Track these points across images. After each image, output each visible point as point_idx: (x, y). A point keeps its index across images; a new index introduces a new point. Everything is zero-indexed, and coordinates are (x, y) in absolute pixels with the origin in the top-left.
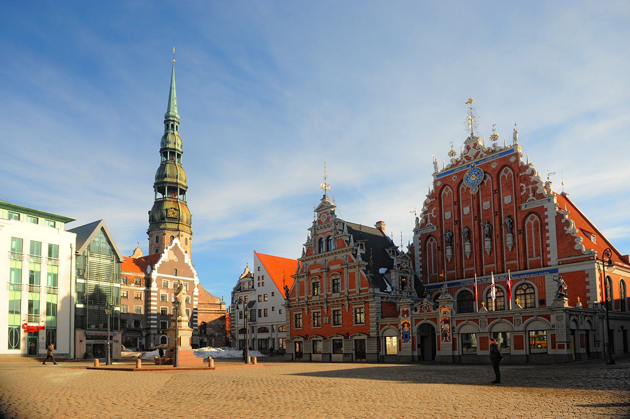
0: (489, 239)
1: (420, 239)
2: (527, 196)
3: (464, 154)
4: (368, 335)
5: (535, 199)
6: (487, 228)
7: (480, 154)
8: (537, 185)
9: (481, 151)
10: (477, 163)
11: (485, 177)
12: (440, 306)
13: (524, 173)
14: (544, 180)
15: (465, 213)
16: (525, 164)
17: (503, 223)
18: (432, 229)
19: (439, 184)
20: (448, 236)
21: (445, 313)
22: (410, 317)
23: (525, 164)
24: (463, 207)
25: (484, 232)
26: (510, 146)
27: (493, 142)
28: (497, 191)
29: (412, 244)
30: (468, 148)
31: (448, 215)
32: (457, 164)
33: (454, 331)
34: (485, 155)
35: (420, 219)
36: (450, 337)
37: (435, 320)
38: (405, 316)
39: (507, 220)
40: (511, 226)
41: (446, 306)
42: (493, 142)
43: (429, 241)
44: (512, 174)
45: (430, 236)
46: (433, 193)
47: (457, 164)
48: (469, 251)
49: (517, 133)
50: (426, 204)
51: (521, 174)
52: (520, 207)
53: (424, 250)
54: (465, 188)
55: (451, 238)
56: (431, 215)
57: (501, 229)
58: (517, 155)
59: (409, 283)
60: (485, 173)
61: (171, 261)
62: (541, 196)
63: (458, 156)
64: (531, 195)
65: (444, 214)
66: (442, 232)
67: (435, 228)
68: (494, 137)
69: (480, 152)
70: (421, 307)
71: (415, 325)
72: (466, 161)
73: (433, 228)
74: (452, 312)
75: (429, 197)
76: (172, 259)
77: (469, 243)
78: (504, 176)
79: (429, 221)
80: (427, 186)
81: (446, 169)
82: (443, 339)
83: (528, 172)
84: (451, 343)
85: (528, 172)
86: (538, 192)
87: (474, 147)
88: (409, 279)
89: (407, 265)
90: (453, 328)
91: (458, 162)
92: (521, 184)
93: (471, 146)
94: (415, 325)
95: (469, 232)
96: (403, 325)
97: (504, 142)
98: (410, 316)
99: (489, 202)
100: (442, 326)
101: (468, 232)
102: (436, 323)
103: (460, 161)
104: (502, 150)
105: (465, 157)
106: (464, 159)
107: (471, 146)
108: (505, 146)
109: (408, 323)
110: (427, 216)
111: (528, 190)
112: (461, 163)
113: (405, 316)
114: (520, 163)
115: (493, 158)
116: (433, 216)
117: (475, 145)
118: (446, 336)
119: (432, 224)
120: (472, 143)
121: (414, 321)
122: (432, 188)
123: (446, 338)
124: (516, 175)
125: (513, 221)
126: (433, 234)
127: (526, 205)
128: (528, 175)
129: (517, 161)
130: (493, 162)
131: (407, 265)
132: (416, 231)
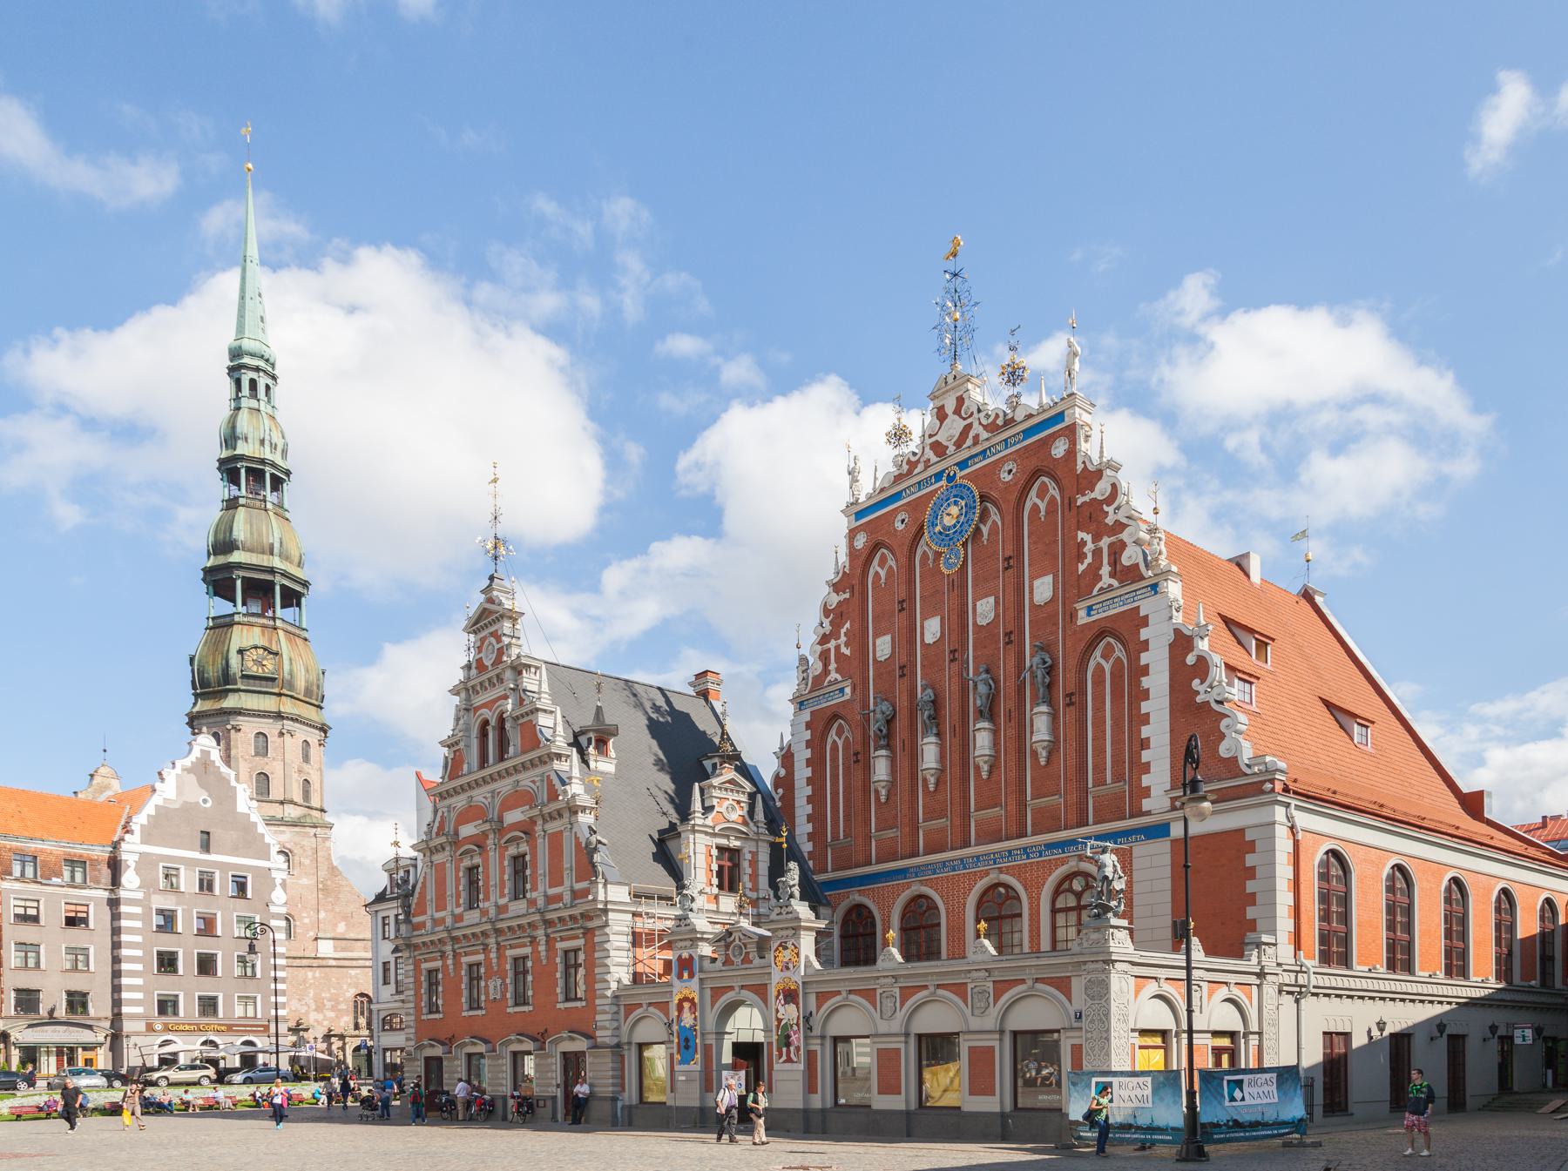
17: (1028, 664)
28: (1013, 562)
33: (811, 1029)
36: (798, 1049)
39: (1037, 660)
40: (1047, 680)
48: (934, 765)
60: (983, 498)
61: (188, 809)
82: (780, 1056)
84: (801, 1067)
90: (807, 1019)
99: (992, 600)
118: (788, 1045)
123: (788, 1052)
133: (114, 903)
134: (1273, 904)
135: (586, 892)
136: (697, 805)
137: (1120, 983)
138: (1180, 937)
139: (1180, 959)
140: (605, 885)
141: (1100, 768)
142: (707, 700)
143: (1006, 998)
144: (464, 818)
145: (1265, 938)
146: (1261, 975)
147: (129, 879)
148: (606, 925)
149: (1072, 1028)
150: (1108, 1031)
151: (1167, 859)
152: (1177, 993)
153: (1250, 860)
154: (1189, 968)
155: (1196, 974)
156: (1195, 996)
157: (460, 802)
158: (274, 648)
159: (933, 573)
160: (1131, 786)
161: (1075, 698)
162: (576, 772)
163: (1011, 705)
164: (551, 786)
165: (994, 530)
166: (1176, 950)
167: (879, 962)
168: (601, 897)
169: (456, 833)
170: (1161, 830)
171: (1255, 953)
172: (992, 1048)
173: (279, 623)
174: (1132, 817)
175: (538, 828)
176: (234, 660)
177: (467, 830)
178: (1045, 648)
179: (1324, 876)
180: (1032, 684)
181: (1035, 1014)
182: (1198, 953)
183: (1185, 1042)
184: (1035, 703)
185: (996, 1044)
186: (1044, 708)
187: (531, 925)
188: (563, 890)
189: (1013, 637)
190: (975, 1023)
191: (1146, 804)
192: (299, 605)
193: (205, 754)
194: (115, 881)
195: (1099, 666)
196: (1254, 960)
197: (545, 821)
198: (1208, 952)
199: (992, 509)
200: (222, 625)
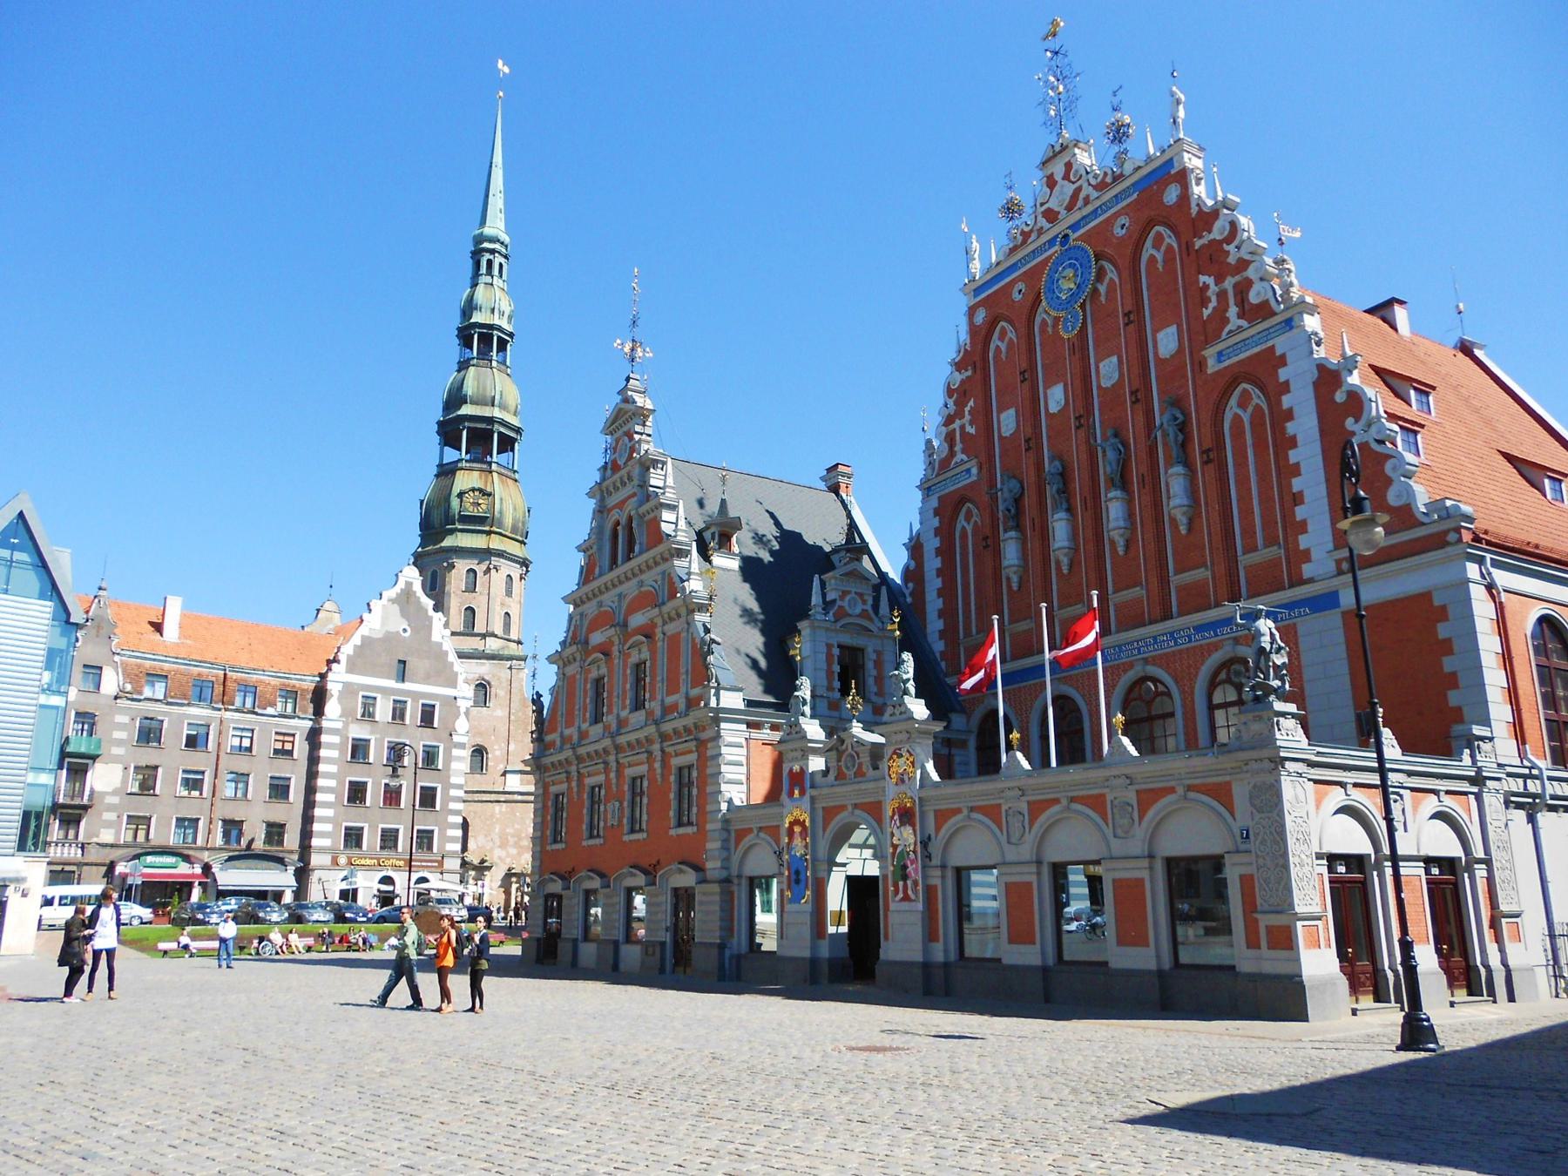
0: (1118, 493)
2: (1220, 317)
4: (699, 868)
5: (1244, 323)
6: (1111, 455)
7: (1082, 195)
8: (1251, 273)
12: (888, 751)
13: (1204, 241)
15: (1054, 408)
16: (1210, 203)
18: (968, 471)
19: (981, 316)
20: (1006, 495)
22: (807, 798)
24: (1046, 388)
28: (1134, 316)
29: (918, 534)
30: (1051, 183)
31: (1007, 422)
32: (1024, 242)
34: (1095, 194)
35: (936, 443)
39: (1166, 417)
40: (1181, 437)
43: (961, 521)
47: (1024, 242)
49: (1178, 102)
50: (950, 392)
51: (1198, 243)
52: (1200, 365)
53: (946, 551)
55: (1018, 501)
56: (962, 427)
57: (1152, 451)
58: (1183, 177)
59: (874, 672)
60: (1098, 257)
61: (390, 639)
62: (1263, 311)
63: (1027, 218)
64: (1233, 311)
66: (992, 483)
67: (974, 471)
68: (1119, 133)
71: (824, 830)
72: (1047, 225)
73: (968, 471)
75: (959, 366)
76: (392, 628)
77: (1062, 515)
78: (1152, 259)
79: (958, 448)
80: (948, 332)
85: (1218, 231)
86: (1253, 298)
87: (1066, 177)
88: (874, 657)
89: (864, 602)
92: (1203, 279)
94: (824, 830)
95: (1064, 475)
96: (791, 833)
98: (809, 792)
99: (1114, 359)
100: (893, 835)
101: (1062, 474)
106: (1042, 222)
109: (802, 824)
111: (1222, 295)
112: (1034, 236)
114: (1193, 205)
117: (1069, 166)
121: (820, 813)
122: (964, 336)
125: (1187, 415)
128: (1220, 242)
129: (1185, 196)
130: (1117, 215)
131: (864, 602)
132: (926, 488)
133: (314, 737)
134: (1481, 686)
135: (700, 698)
136: (816, 599)
137: (1295, 791)
138: (1367, 735)
139: (1368, 758)
140: (718, 689)
141: (1249, 532)
142: (837, 494)
144: (593, 627)
145: (1477, 730)
146: (1478, 780)
147: (332, 708)
148: (718, 736)
149: (1238, 851)
150: (1285, 855)
151: (1340, 637)
152: (1370, 802)
153: (1443, 630)
154: (1382, 771)
155: (1393, 778)
156: (1396, 809)
158: (489, 490)
159: (1053, 341)
160: (1287, 550)
161: (1214, 455)
162: (695, 568)
163: (1144, 469)
164: (672, 584)
166: (1364, 745)
168: (713, 703)
169: (587, 642)
170: (1327, 601)
171: (1467, 751)
172: (1140, 881)
173: (494, 467)
174: (1292, 586)
175: (658, 631)
176: (455, 503)
177: (597, 638)
178: (1178, 403)
179: (1540, 650)
180: (1165, 444)
181: (1193, 833)
182: (1392, 750)
183: (1389, 871)
184: (1168, 465)
185: (1145, 874)
186: (1179, 469)
187: (649, 740)
188: (678, 699)
189: (1141, 395)
190: (1117, 847)
191: (1307, 570)
192: (512, 450)
193: (409, 584)
194: (319, 711)
195: (1237, 420)
196: (1467, 760)
197: (665, 623)
198: (1407, 747)
199: (1108, 266)
200: (447, 472)
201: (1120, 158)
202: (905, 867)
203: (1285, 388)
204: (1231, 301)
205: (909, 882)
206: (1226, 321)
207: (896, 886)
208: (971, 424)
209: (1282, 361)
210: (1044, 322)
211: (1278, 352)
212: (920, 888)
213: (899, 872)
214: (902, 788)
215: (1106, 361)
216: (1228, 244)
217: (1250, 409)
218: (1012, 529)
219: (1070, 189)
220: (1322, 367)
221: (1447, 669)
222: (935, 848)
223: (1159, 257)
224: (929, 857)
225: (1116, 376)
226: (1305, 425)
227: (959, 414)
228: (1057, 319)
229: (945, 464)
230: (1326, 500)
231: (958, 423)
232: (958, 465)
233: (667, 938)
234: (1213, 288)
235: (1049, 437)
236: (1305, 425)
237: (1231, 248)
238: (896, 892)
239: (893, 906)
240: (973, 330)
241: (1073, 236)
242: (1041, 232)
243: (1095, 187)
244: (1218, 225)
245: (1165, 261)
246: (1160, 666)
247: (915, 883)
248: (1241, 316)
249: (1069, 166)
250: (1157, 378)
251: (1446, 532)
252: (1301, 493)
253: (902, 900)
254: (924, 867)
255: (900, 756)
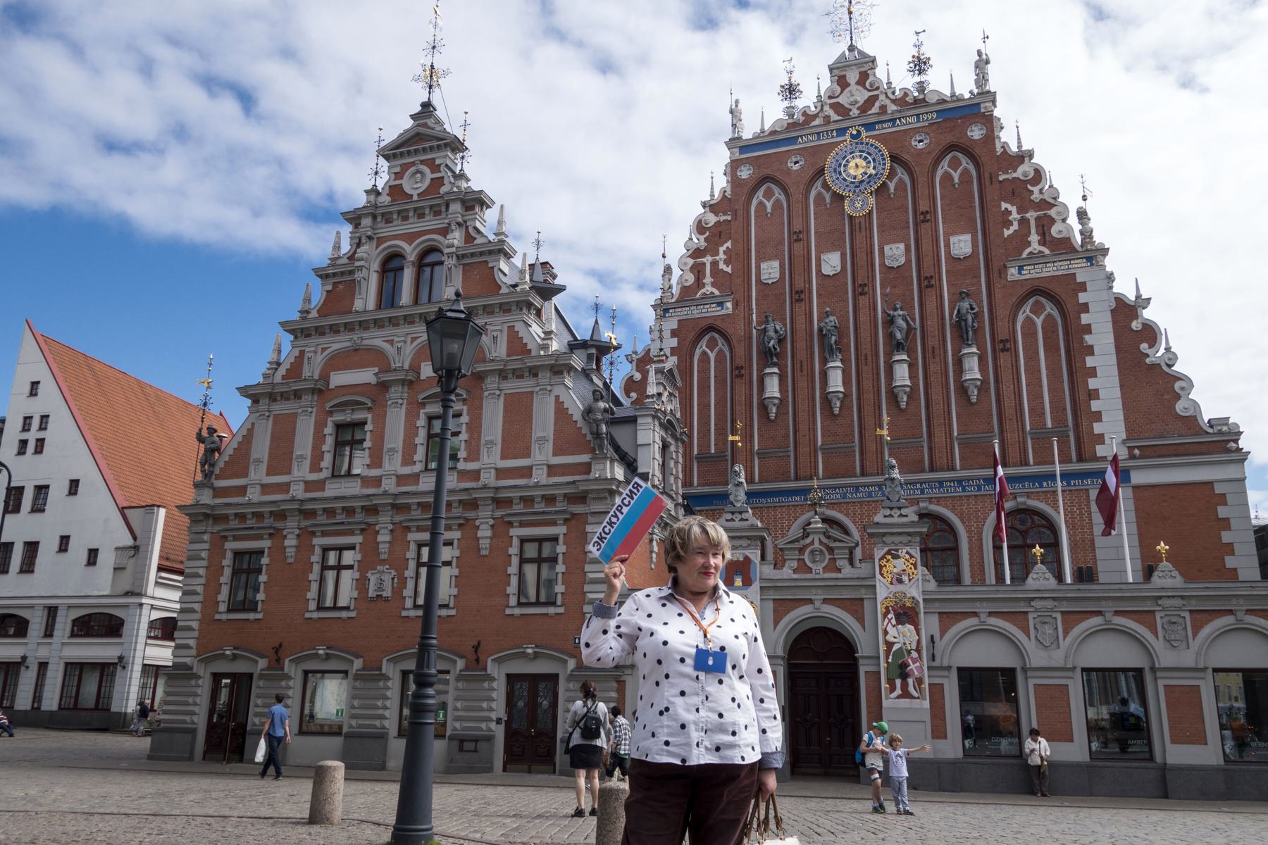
1: (674, 333)
2: (1021, 239)
3: (830, 97)
4: (576, 654)
5: (1047, 252)
7: (877, 104)
8: (1053, 212)
9: (882, 97)
10: (869, 126)
11: (892, 174)
13: (1009, 177)
14: (1070, 199)
15: (827, 270)
19: (745, 173)
21: (900, 581)
22: (756, 586)
23: (1014, 148)
25: (890, 336)
26: (971, 92)
27: (917, 79)
28: (924, 218)
30: (842, 82)
34: (894, 108)
35: (677, 273)
37: (855, 606)
38: (738, 582)
41: (902, 553)
42: (917, 79)
43: (703, 346)
44: (974, 173)
45: (711, 328)
46: (724, 197)
49: (987, 62)
50: (700, 227)
51: (1001, 178)
54: (828, 197)
56: (715, 264)
58: (989, 122)
60: (894, 158)
62: (1063, 246)
63: (807, 100)
64: (1034, 238)
65: (758, 267)
67: (729, 305)
68: (920, 65)
69: (876, 97)
70: (802, 550)
72: (835, 117)
73: (721, 304)
74: (925, 581)
77: (839, 364)
78: (947, 177)
79: (708, 280)
80: (708, 175)
81: (773, 133)
83: (1023, 171)
85: (1023, 171)
91: (808, 117)
92: (1004, 205)
93: (852, 77)
97: (951, 79)
99: (902, 246)
100: (886, 633)
102: (861, 620)
103: (816, 116)
104: (944, 101)
105: (832, 106)
106: (828, 111)
107: (852, 77)
108: (953, 95)
110: (704, 264)
111: (1024, 222)
112: (817, 122)
113: (738, 582)
114: (998, 146)
115: (918, 121)
116: (722, 266)
117: (864, 77)
119: (717, 293)
120: (854, 69)
121: (770, 605)
122: (722, 182)
124: (987, 175)
125: (981, 307)
126: (719, 323)
127: (1021, 268)
128: (1026, 182)
129: (990, 137)
141: (1037, 412)
143: (1206, 630)
157: (338, 343)
161: (1004, 345)
165: (901, 186)
167: (1030, 580)
191: (1101, 451)
195: (1029, 323)
201: (921, 87)
202: (904, 665)
203: (1085, 308)
204: (1033, 230)
205: (910, 681)
206: (1029, 244)
207: (891, 682)
208: (727, 262)
209: (1083, 287)
210: (819, 195)
211: (1079, 280)
212: (926, 686)
213: (898, 672)
214: (900, 588)
215: (893, 246)
216: (1033, 185)
217: (1042, 317)
218: (774, 365)
219: (862, 96)
220: (1120, 300)
221: (1225, 540)
222: (940, 645)
223: (956, 176)
224: (933, 658)
225: (903, 260)
226: (1102, 339)
227: (711, 248)
228: (839, 198)
229: (685, 291)
230: (1120, 401)
231: (708, 260)
232: (705, 297)
233: (499, 732)
234: (1015, 215)
235: (819, 295)
236: (1102, 339)
237: (1036, 189)
238: (893, 689)
239: (885, 703)
240: (735, 181)
241: (864, 135)
242: (827, 120)
243: (893, 101)
244: (1021, 169)
245: (961, 182)
246: (946, 507)
247: (919, 681)
248: (1043, 242)
249: (864, 77)
250: (947, 271)
251: (1229, 441)
252: (1097, 390)
253: (899, 697)
254: (929, 668)
255: (896, 557)
